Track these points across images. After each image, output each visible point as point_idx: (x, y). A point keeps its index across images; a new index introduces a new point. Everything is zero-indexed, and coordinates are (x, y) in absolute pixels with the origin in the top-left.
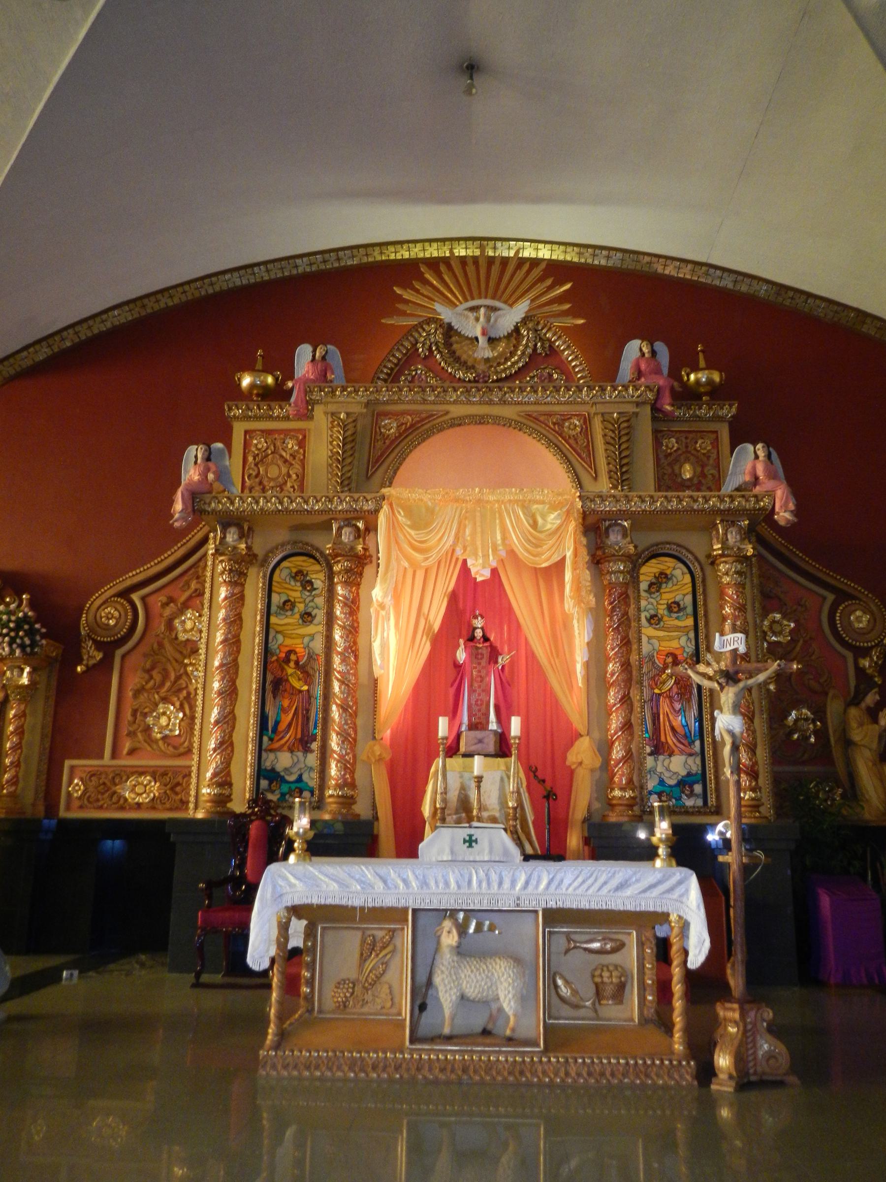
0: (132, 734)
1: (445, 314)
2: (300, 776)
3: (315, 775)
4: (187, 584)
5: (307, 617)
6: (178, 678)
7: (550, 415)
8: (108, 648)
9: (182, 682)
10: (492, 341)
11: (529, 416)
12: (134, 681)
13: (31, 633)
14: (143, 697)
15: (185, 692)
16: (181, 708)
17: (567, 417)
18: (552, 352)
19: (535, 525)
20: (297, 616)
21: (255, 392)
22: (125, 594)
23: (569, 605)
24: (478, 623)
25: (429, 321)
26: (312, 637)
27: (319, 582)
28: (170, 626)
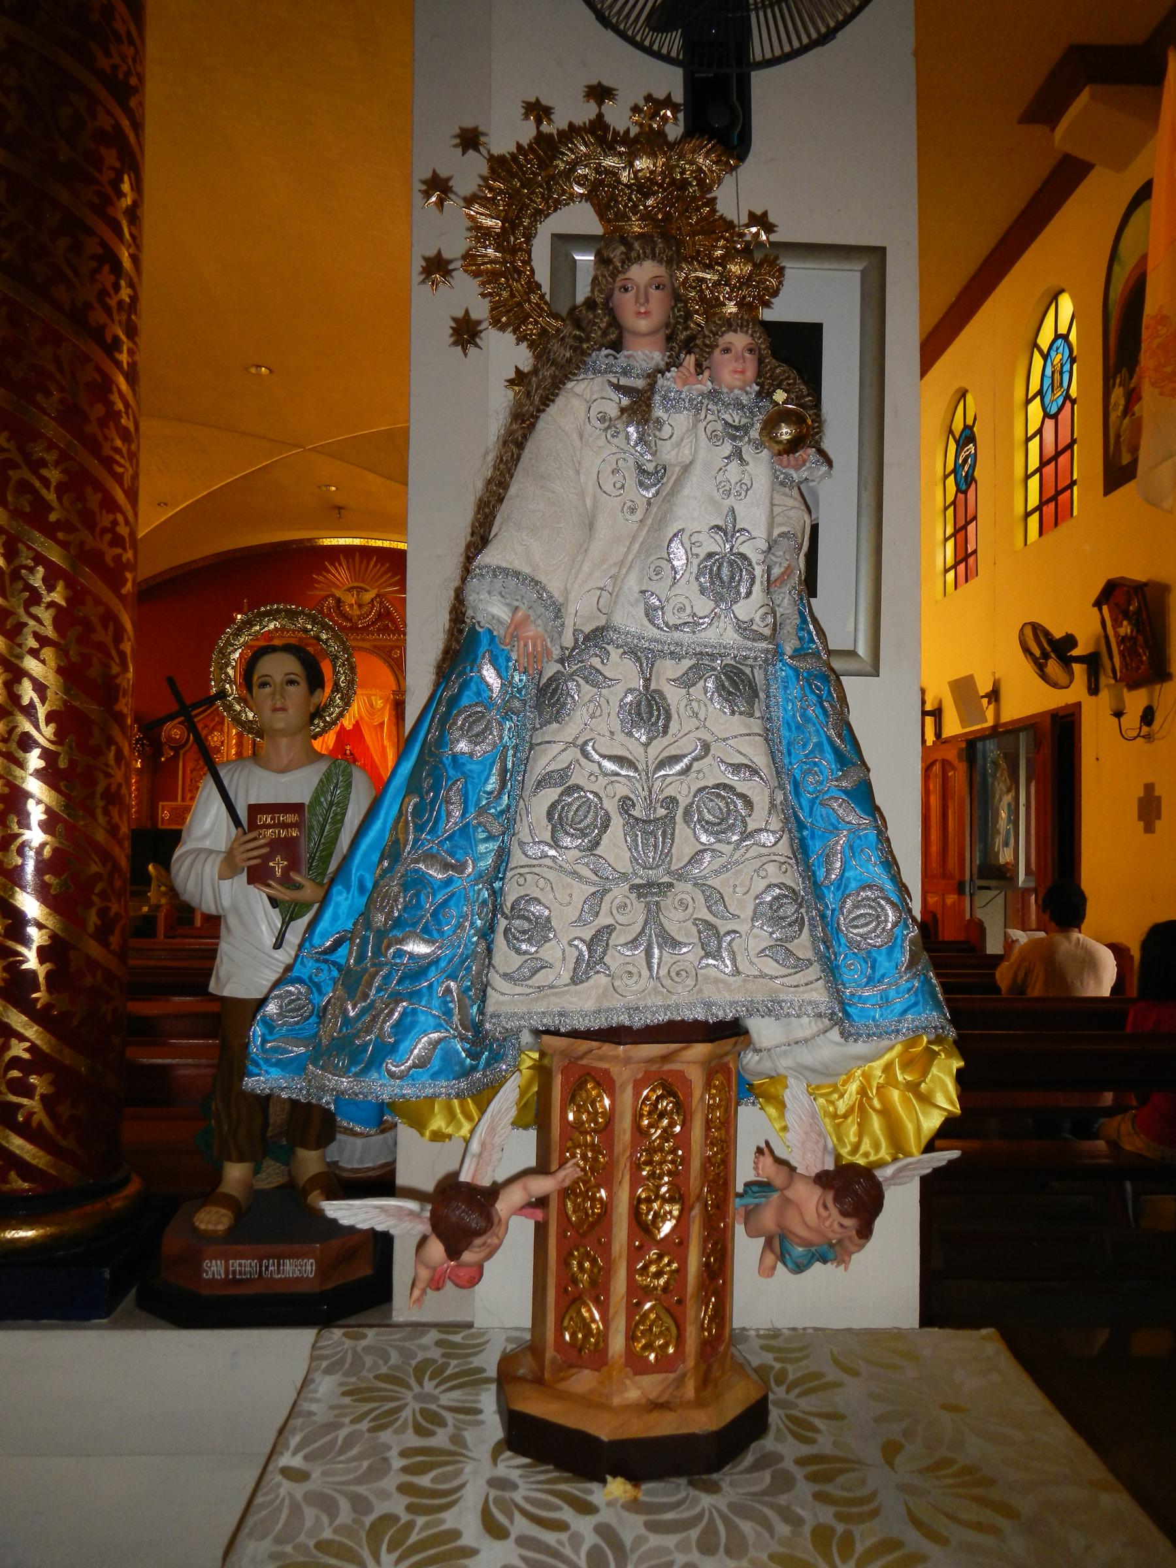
0: (190, 791)
1: (338, 594)
4: (213, 719)
7: (384, 647)
8: (177, 750)
10: (360, 606)
11: (375, 647)
12: (191, 765)
13: (143, 745)
14: (195, 773)
17: (392, 648)
18: (389, 613)
19: (372, 706)
23: (386, 742)
24: (348, 747)
25: (328, 596)
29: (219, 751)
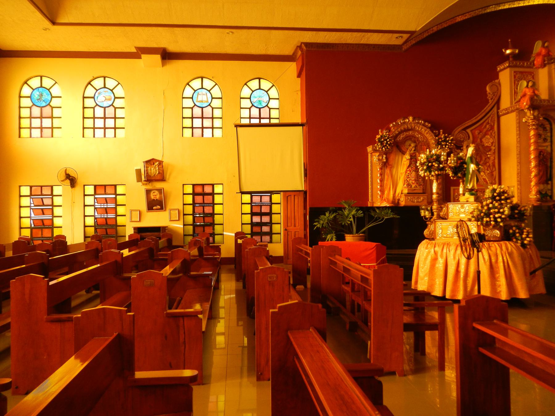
2: (546, 192)
3: (550, 191)
4: (485, 126)
5: (545, 140)
6: (485, 159)
9: (487, 160)
15: (488, 164)
16: (487, 170)
20: (542, 139)
21: (510, 56)
22: (465, 129)
26: (547, 146)
27: (548, 128)
28: (481, 141)
29: (490, 150)
